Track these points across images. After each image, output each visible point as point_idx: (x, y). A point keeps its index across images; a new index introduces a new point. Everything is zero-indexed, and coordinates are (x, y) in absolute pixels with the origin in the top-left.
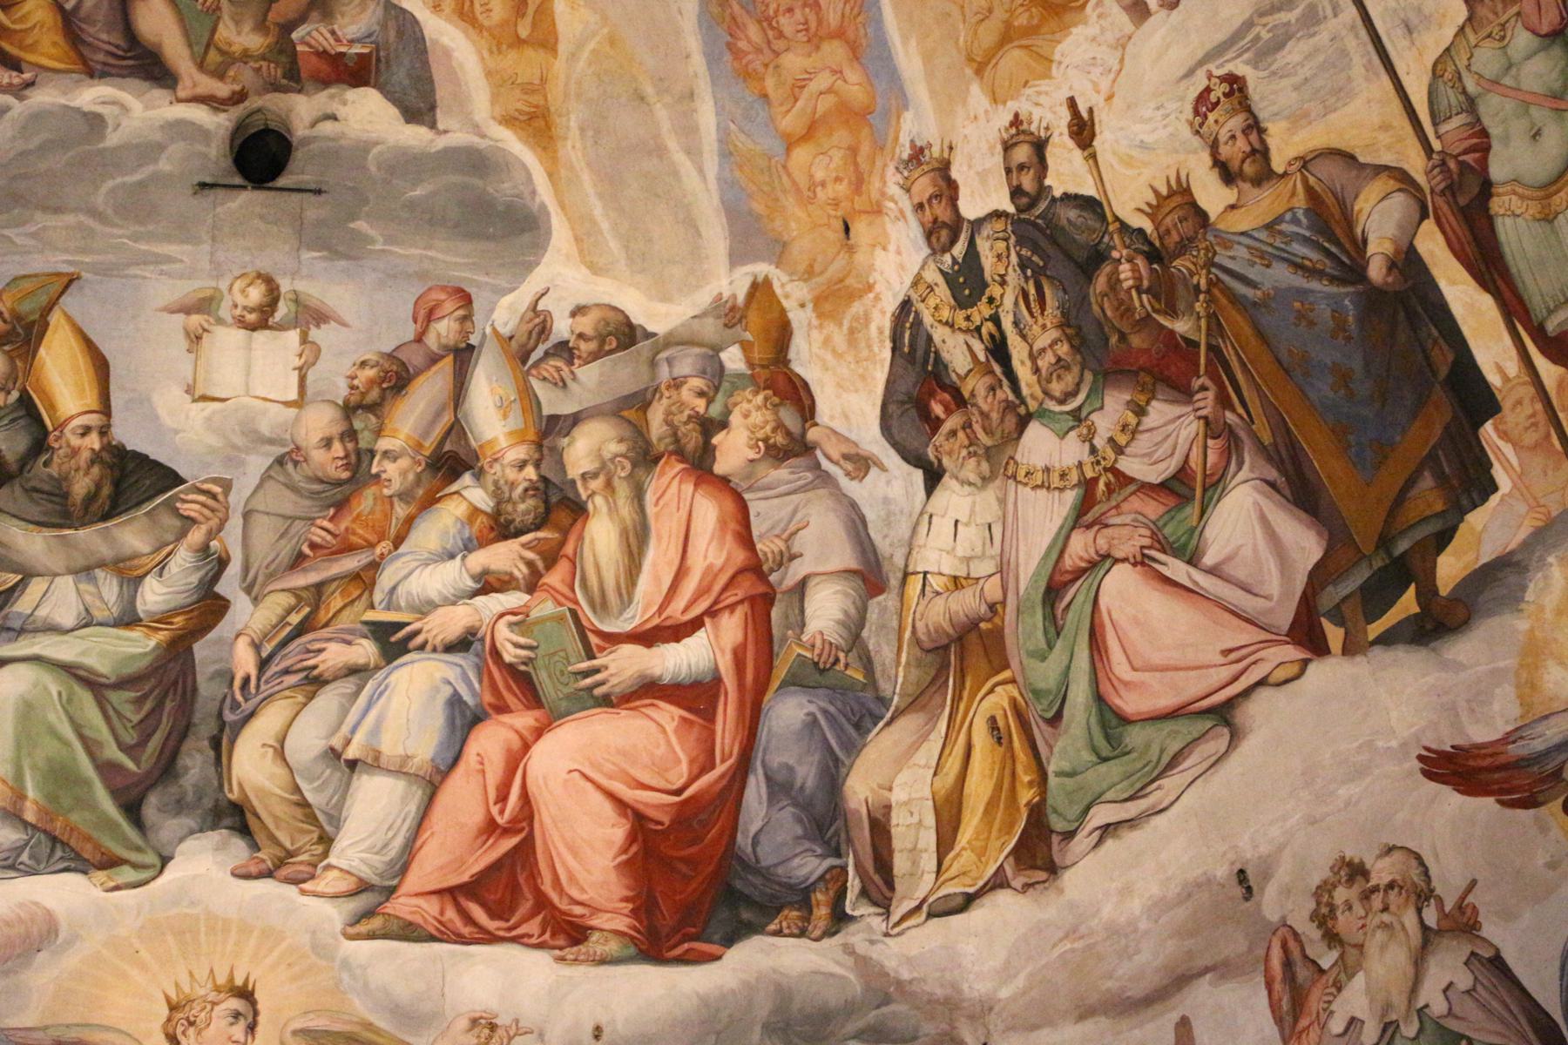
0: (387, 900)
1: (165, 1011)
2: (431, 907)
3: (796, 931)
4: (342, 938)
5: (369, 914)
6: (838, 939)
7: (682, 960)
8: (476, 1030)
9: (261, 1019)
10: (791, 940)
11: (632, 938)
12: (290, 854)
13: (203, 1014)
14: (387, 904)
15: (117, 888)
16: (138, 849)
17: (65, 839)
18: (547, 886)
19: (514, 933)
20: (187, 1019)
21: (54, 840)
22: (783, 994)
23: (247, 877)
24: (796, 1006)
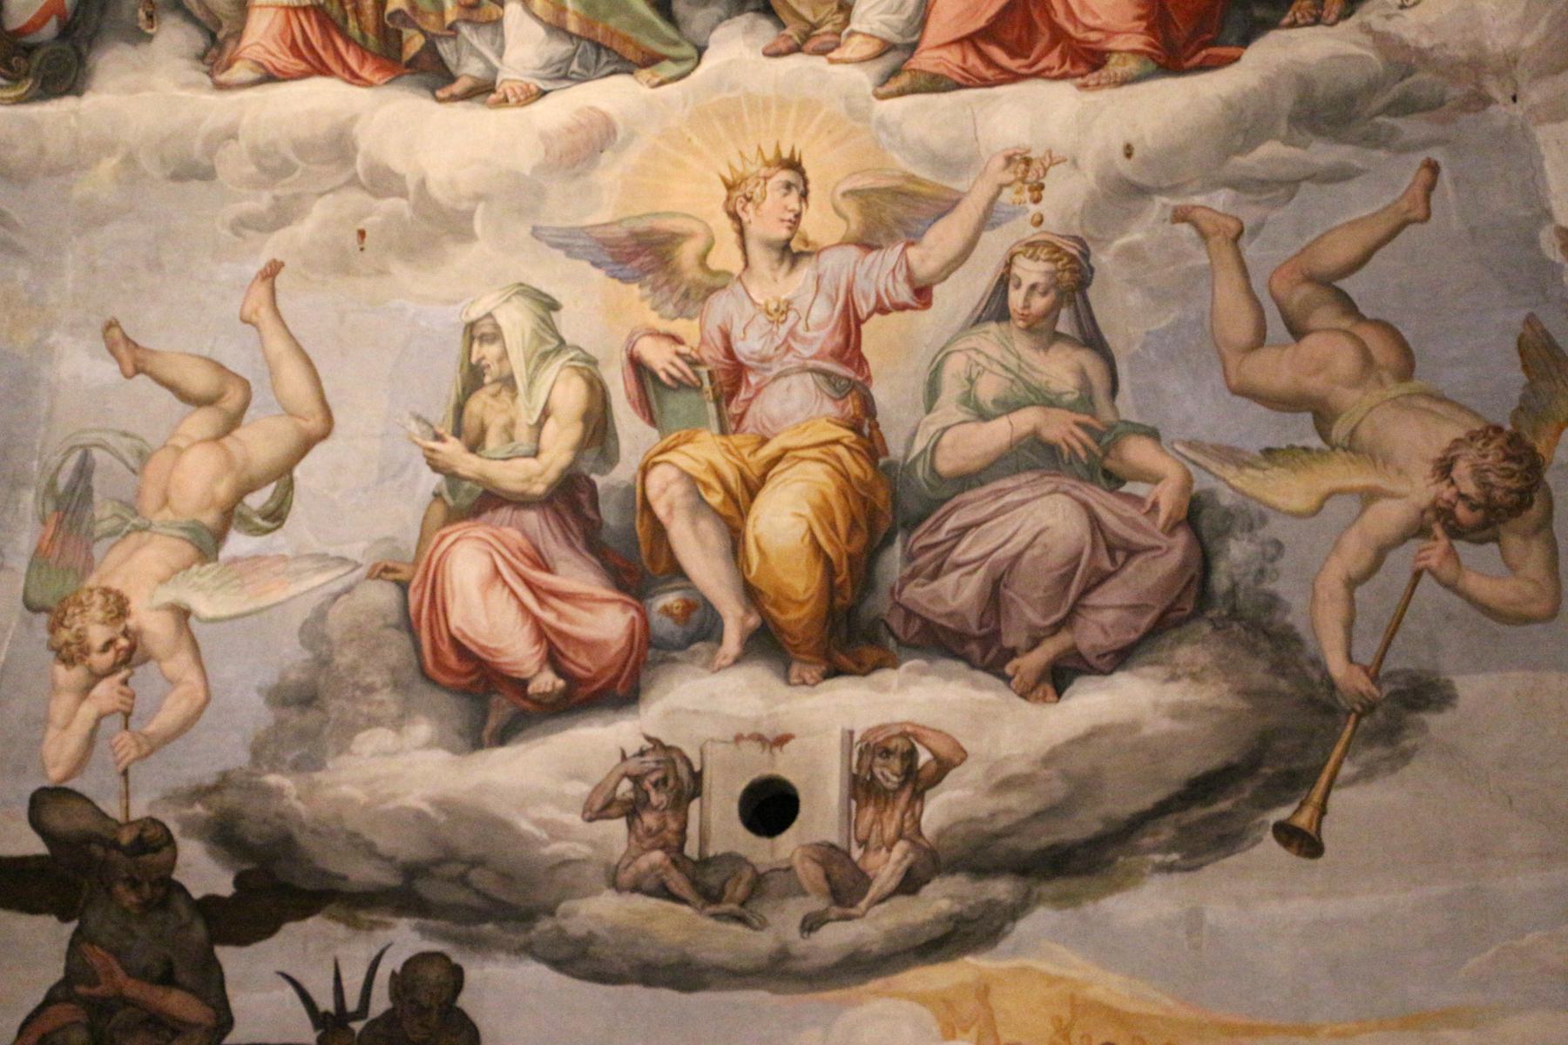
0: (911, 55)
1: (723, 192)
2: (953, 56)
3: (1311, 20)
4: (874, 99)
5: (895, 72)
6: (1354, 20)
7: (1202, 68)
8: (1012, 168)
9: (811, 186)
10: (1307, 29)
11: (1150, 55)
12: (814, 27)
13: (758, 190)
14: (912, 60)
15: (661, 83)
16: (676, 44)
17: (607, 43)
18: (1061, 19)
19: (1034, 69)
20: (745, 196)
21: (598, 46)
22: (1304, 84)
23: (778, 54)
24: (1320, 90)
